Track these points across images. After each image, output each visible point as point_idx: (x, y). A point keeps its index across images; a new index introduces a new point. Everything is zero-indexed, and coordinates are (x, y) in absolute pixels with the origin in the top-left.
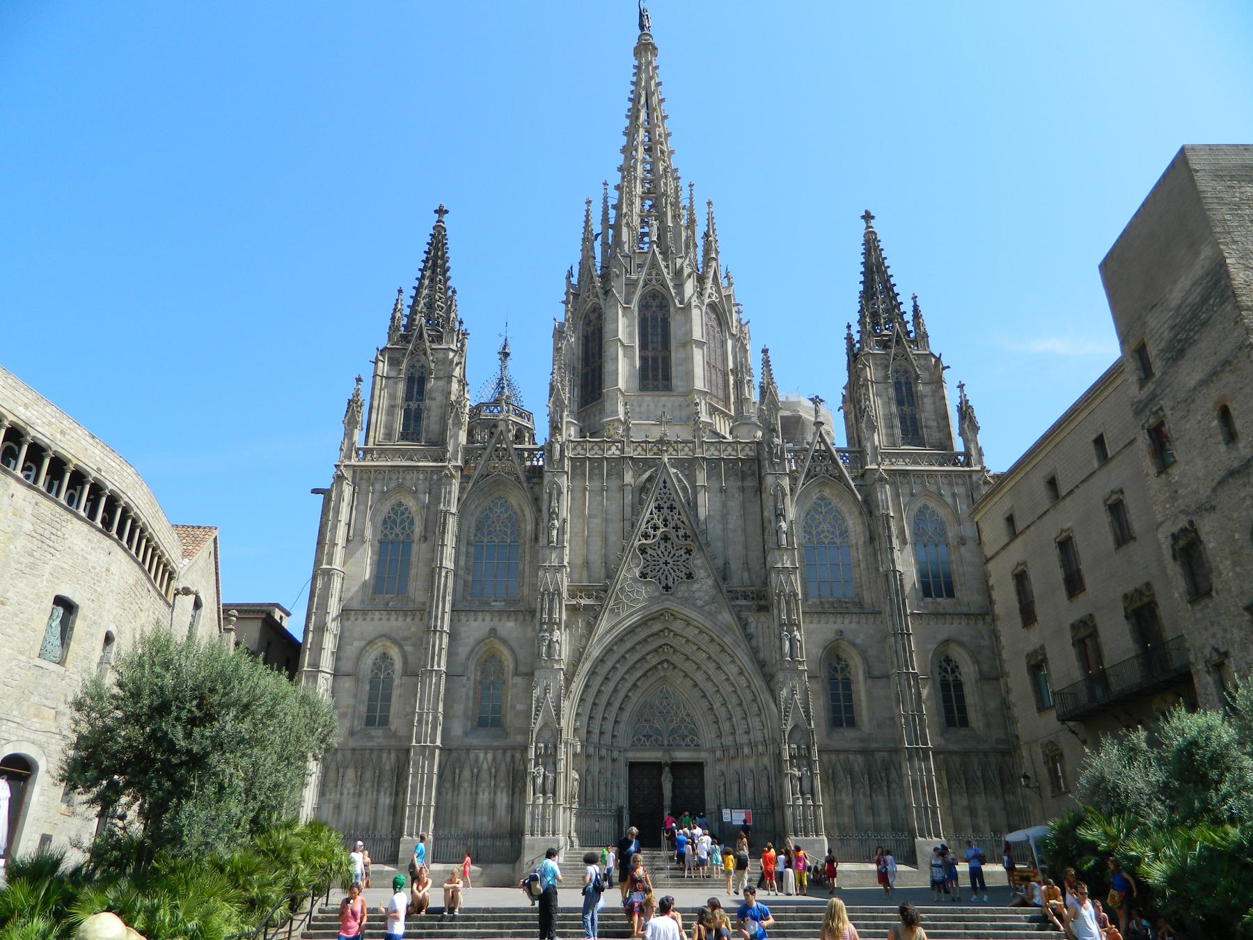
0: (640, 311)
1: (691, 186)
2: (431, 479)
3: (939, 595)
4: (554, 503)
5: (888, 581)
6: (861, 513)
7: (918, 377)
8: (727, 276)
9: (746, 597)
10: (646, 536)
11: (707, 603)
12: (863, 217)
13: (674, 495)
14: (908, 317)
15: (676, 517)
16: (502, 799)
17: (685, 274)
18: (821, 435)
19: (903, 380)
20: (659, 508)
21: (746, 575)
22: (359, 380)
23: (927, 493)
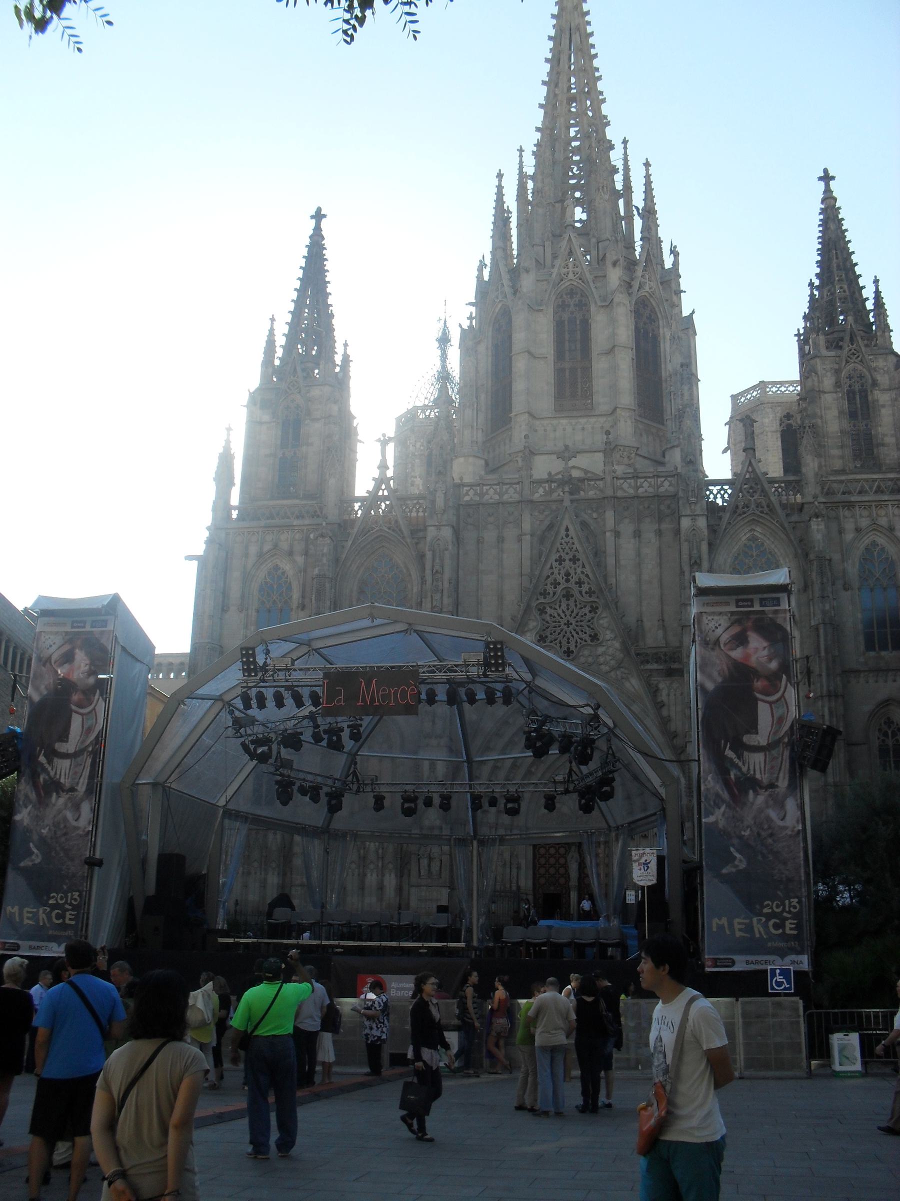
0: (555, 313)
1: (625, 142)
2: (308, 538)
3: (884, 647)
4: (437, 561)
5: (818, 636)
6: (796, 556)
7: (875, 383)
8: (672, 252)
9: (657, 659)
10: (544, 594)
11: (613, 669)
12: (820, 179)
13: (577, 545)
14: (870, 305)
15: (579, 571)
16: (390, 881)
17: (609, 263)
18: (750, 464)
19: (857, 387)
20: (560, 561)
21: (661, 633)
22: (229, 429)
23: (875, 527)
